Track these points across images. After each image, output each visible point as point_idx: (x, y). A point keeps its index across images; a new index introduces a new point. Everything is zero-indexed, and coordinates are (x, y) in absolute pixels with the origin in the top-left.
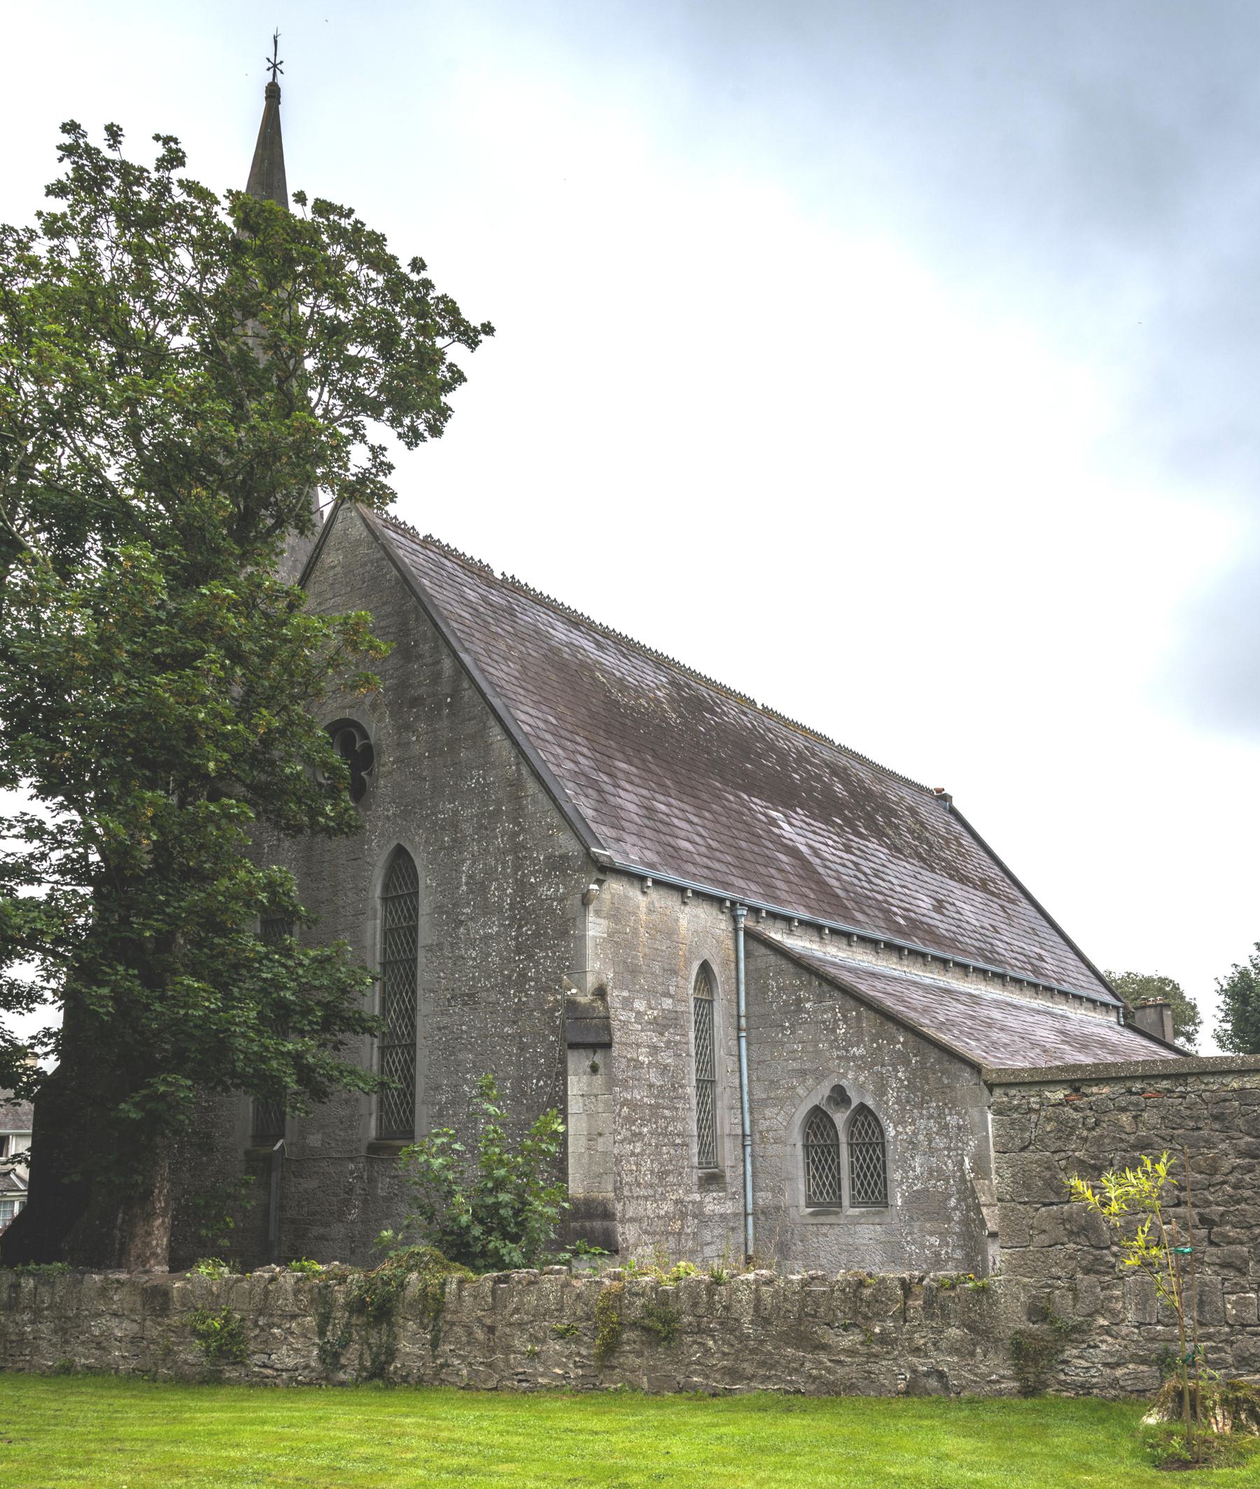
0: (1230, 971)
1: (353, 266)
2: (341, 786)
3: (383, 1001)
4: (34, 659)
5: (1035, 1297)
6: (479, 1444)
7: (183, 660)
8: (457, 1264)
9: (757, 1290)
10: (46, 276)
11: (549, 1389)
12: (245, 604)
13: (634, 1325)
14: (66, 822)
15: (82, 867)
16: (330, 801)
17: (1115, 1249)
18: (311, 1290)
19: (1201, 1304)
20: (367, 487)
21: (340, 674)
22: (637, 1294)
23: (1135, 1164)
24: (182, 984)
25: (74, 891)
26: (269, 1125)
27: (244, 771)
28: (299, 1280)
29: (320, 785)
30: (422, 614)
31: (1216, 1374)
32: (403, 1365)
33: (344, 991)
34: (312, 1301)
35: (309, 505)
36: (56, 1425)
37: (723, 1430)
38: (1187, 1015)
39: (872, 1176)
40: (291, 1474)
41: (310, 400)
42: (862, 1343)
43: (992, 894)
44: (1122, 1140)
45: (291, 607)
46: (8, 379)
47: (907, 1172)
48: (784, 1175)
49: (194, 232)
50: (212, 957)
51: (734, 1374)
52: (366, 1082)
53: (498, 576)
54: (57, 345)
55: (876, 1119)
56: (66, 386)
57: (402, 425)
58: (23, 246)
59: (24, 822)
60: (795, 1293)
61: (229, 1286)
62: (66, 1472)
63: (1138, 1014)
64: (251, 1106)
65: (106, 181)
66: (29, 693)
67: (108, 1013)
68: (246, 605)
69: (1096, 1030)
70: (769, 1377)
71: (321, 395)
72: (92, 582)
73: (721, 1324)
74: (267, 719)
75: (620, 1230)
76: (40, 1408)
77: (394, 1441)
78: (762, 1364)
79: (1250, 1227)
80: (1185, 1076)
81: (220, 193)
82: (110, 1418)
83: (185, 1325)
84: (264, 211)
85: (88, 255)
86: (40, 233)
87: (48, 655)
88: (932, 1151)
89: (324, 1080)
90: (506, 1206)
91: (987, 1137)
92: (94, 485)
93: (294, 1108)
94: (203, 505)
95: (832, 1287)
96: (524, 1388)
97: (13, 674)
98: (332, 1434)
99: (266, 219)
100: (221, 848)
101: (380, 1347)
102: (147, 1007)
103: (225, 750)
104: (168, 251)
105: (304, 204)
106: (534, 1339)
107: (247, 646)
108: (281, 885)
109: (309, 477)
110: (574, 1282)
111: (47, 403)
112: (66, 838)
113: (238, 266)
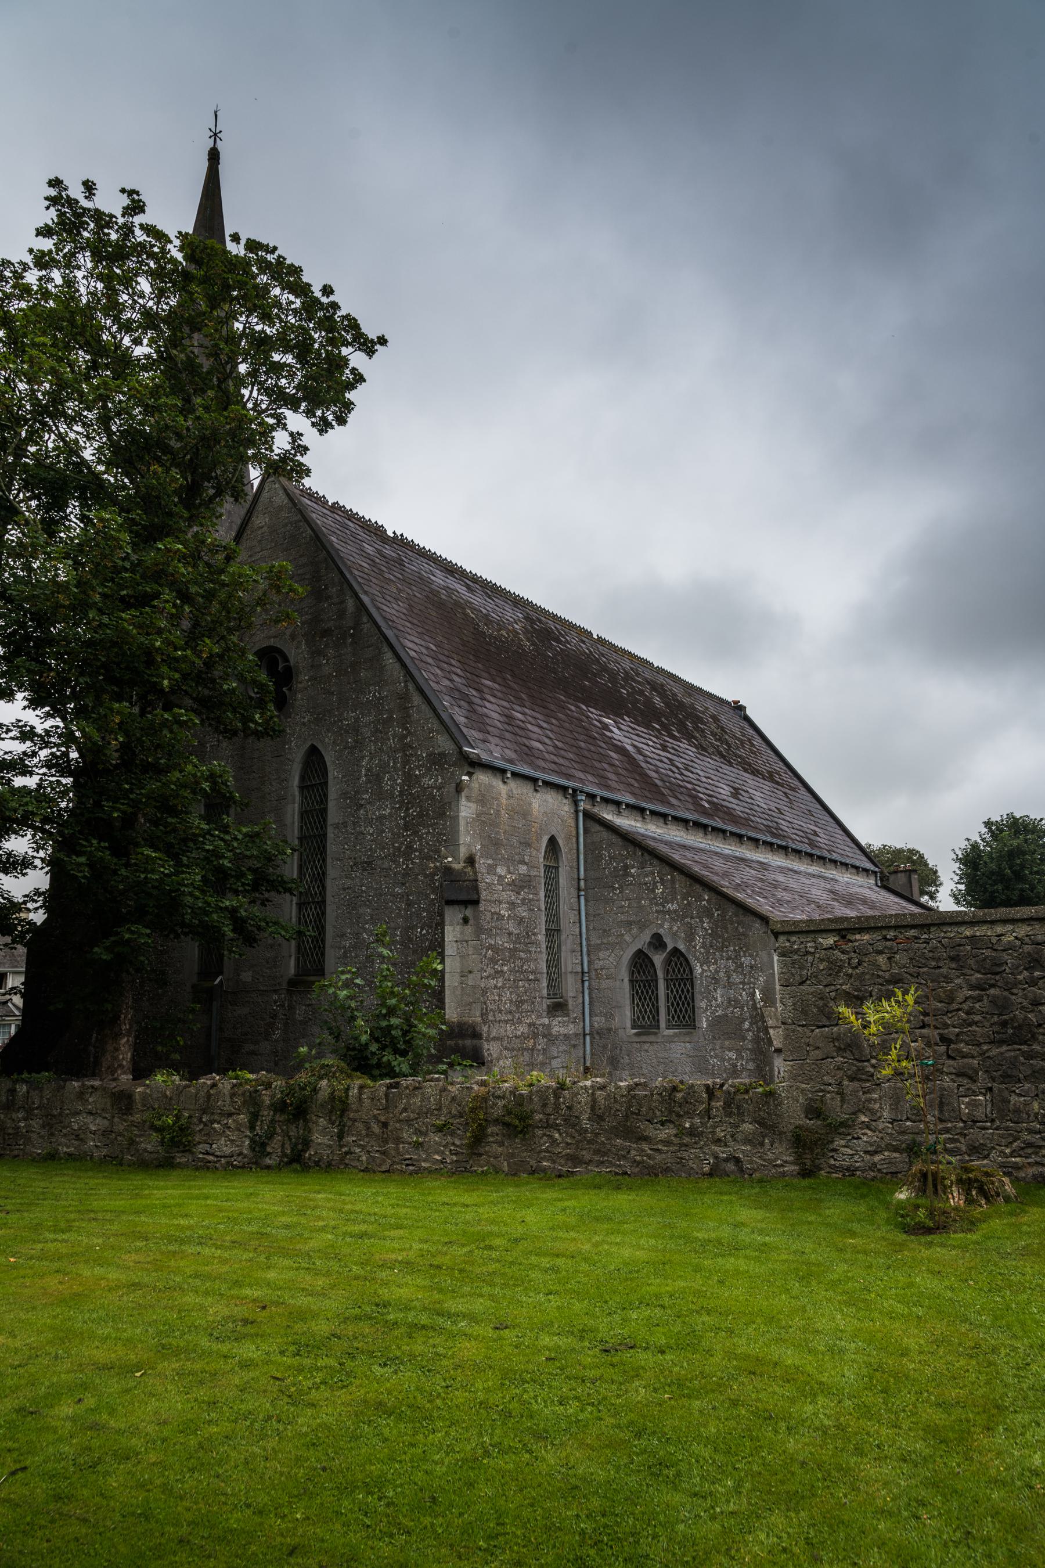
0: (964, 844)
1: (277, 291)
2: (267, 699)
3: (300, 867)
4: (27, 599)
5: (811, 1099)
6: (375, 1214)
7: (143, 600)
8: (358, 1074)
9: (593, 1094)
10: (36, 299)
11: (430, 1171)
12: (192, 556)
13: (497, 1121)
14: (52, 727)
15: (64, 762)
16: (259, 711)
17: (874, 1061)
18: (243, 1094)
19: (941, 1104)
20: (288, 464)
21: (266, 611)
22: (499, 1097)
23: (889, 996)
24: (142, 854)
25: (58, 781)
26: (211, 965)
27: (191, 687)
28: (234, 1086)
29: (251, 698)
30: (340, 567)
31: (953, 1160)
32: (316, 1153)
33: (269, 859)
34: (244, 1103)
35: (243, 478)
36: (44, 1199)
37: (567, 1203)
38: (930, 878)
39: (683, 1004)
40: (228, 1238)
41: (243, 396)
42: (675, 1136)
43: (777, 783)
44: (879, 976)
45: (228, 559)
46: (6, 379)
47: (710, 1001)
48: (614, 1004)
49: (152, 264)
50: (166, 833)
51: (575, 1160)
52: (286, 931)
53: (390, 534)
54: (45, 353)
55: (687, 960)
56: (51, 385)
57: (315, 416)
58: (18, 276)
59: (18, 727)
60: (623, 1096)
61: (179, 1091)
62: (52, 1236)
63: (892, 878)
64: (197, 949)
65: (83, 225)
66: (23, 625)
67: (85, 877)
68: (193, 557)
69: (858, 890)
70: (602, 1162)
71: (251, 392)
72: (72, 539)
73: (565, 1120)
74: (209, 646)
75: (486, 1046)
76: (31, 1186)
77: (309, 1212)
78: (597, 1152)
79: (979, 1045)
80: (929, 926)
81: (172, 234)
82: (86, 1194)
83: (145, 1122)
84: (206, 248)
85: (69, 283)
86: (31, 265)
87: (38, 596)
88: (730, 985)
89: (255, 929)
90: (397, 1028)
91: (773, 974)
92: (74, 463)
93: (231, 951)
94: (159, 478)
95: (652, 1092)
96: (411, 1171)
97: (11, 611)
98: (260, 1206)
99: (209, 255)
100: (173, 747)
101: (298, 1138)
102: (115, 872)
103: (176, 671)
104: (131, 279)
105: (238, 243)
106: (418, 1132)
107: (193, 589)
108: (221, 776)
109: (242, 457)
110: (450, 1088)
111: (37, 398)
112: (52, 739)
113: (187, 291)
